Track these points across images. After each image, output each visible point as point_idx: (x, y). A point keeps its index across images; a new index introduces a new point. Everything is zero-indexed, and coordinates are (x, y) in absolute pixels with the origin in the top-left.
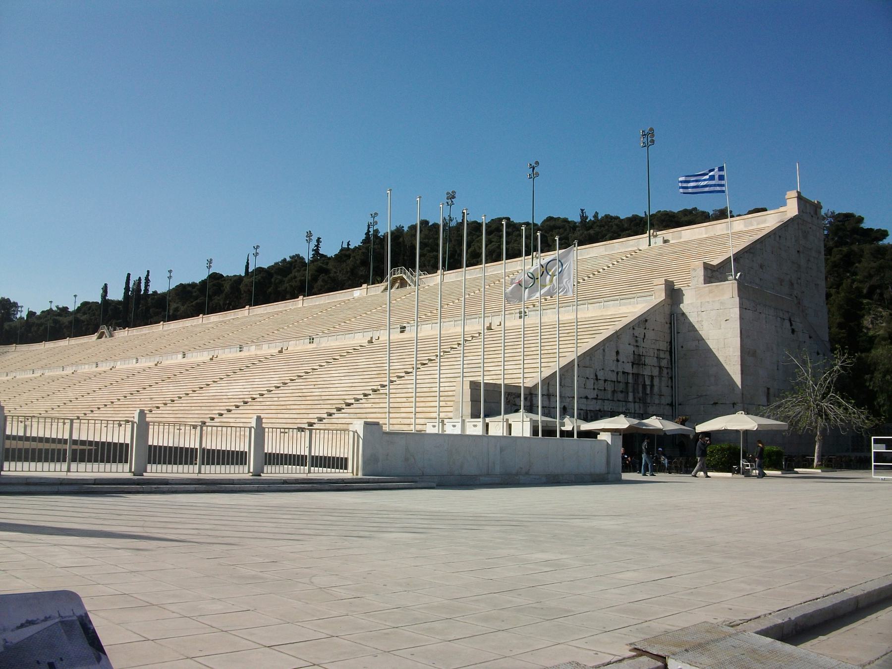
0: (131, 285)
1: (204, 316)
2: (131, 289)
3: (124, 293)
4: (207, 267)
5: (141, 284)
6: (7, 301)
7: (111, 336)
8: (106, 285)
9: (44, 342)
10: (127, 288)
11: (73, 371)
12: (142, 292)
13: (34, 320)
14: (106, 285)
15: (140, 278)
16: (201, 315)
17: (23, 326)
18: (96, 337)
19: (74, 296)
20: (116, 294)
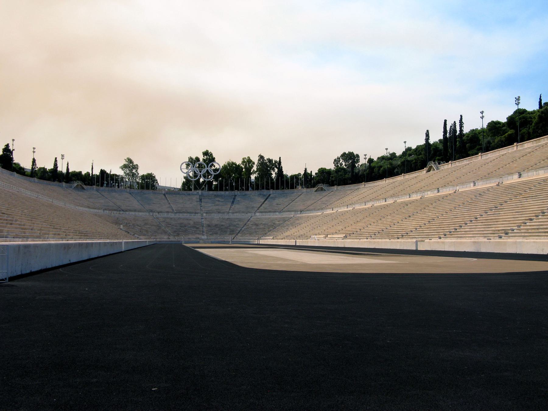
0: (448, 129)
1: (518, 144)
2: (448, 131)
3: (443, 135)
4: (516, 103)
5: (456, 127)
6: (352, 154)
7: (438, 169)
8: (428, 131)
9: (384, 179)
10: (445, 131)
11: (394, 201)
12: (458, 132)
13: (372, 165)
14: (428, 131)
15: (455, 122)
16: (515, 144)
17: (368, 169)
18: (425, 172)
19: (404, 142)
20: (436, 137)
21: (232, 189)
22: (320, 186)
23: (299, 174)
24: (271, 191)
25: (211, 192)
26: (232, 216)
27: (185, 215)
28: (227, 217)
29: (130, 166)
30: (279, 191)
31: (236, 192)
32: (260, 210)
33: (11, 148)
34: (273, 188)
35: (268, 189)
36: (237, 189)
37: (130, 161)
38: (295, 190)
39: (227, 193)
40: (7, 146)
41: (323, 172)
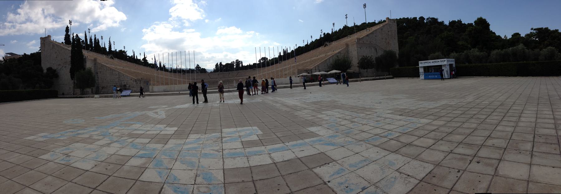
21: (229, 71)
22: (254, 68)
23: (248, 65)
24: (240, 71)
25: (221, 73)
26: (228, 79)
27: (215, 80)
28: (227, 79)
29: (198, 67)
30: (242, 71)
31: (230, 72)
32: (237, 76)
33: (165, 65)
34: (240, 70)
35: (239, 70)
36: (230, 71)
37: (199, 65)
38: (247, 70)
39: (227, 72)
40: (164, 65)
41: (254, 64)
